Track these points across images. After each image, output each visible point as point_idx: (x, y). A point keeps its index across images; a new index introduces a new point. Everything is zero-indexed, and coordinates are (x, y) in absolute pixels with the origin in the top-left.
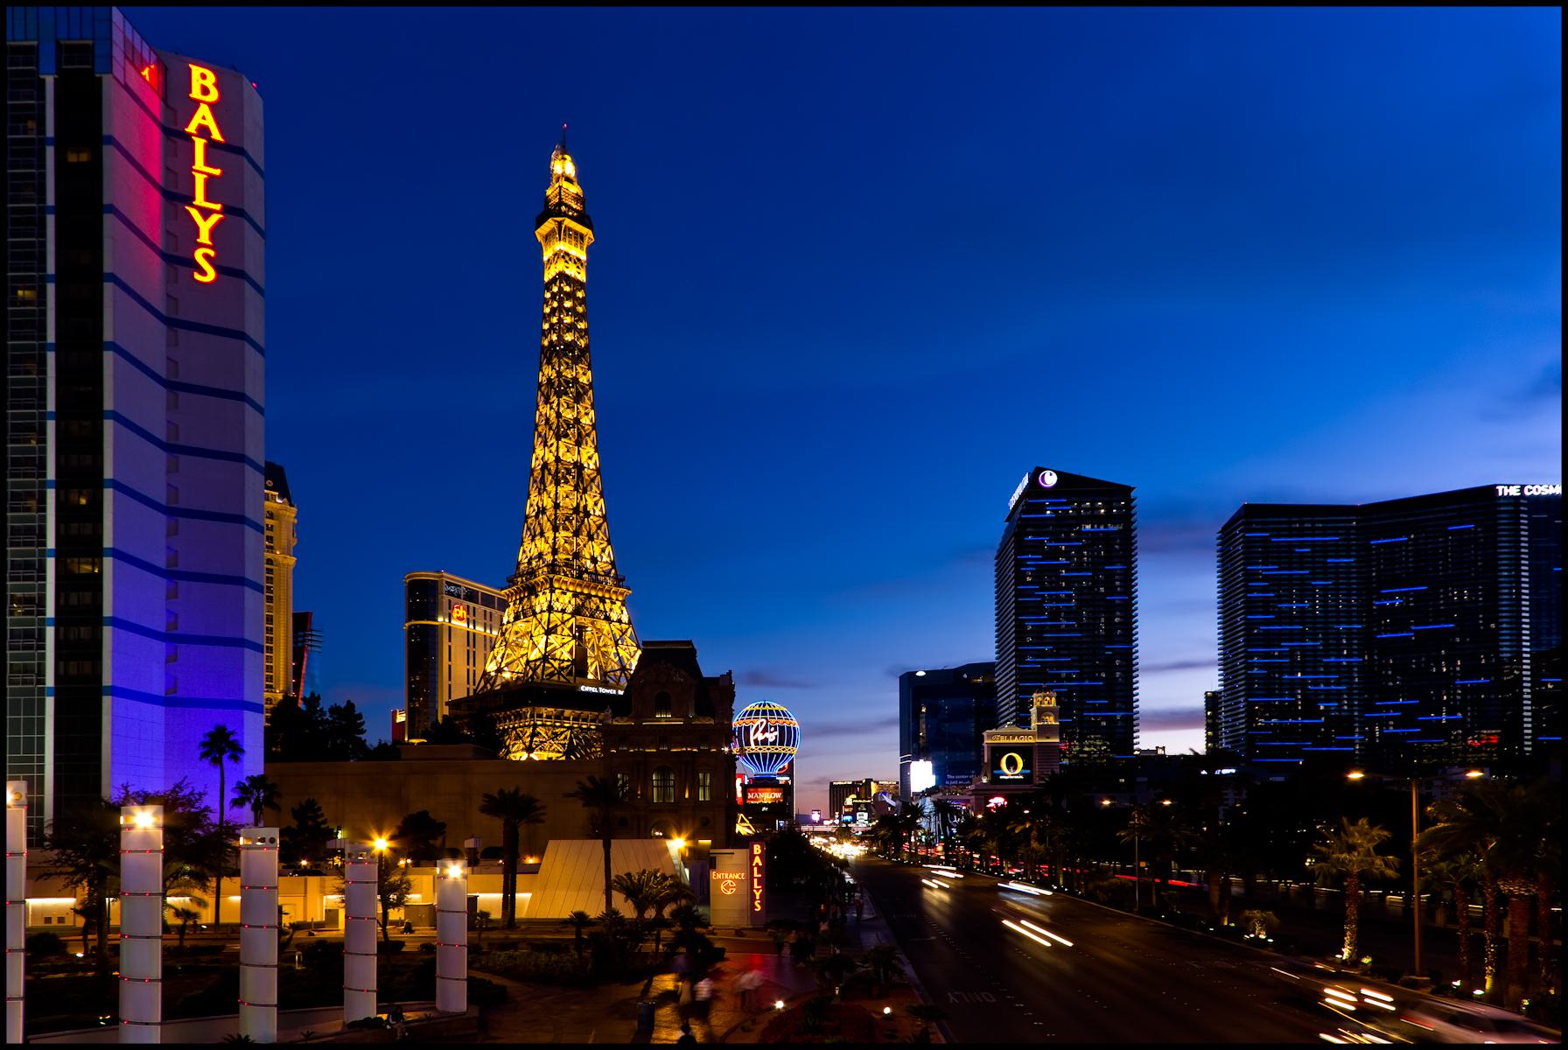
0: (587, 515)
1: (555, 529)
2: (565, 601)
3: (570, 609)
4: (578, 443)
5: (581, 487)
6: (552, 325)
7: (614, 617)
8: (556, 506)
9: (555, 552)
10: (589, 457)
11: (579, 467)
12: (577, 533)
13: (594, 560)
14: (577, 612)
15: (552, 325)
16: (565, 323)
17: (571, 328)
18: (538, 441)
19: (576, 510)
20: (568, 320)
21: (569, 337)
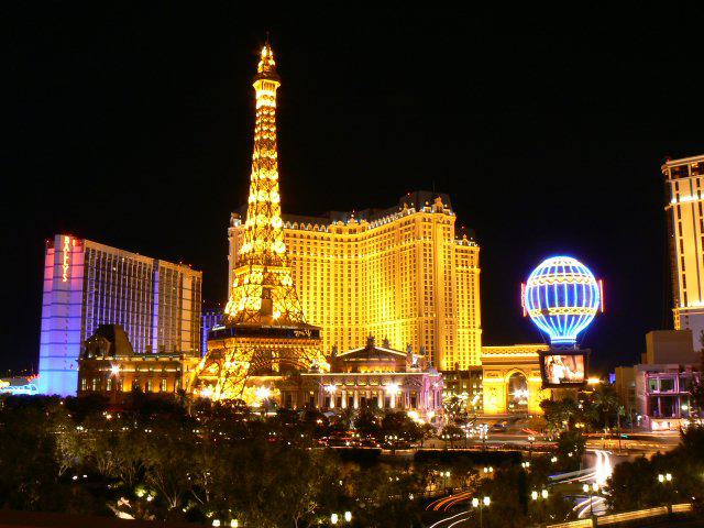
0: (272, 228)
1: (255, 239)
2: (259, 278)
3: (260, 282)
4: (268, 191)
5: (269, 213)
7: (284, 283)
8: (256, 226)
9: (254, 251)
10: (275, 198)
11: (269, 204)
12: (266, 240)
13: (275, 253)
14: (263, 284)
16: (266, 130)
17: (268, 131)
18: (251, 190)
19: (266, 227)
20: (265, 128)
21: (265, 137)
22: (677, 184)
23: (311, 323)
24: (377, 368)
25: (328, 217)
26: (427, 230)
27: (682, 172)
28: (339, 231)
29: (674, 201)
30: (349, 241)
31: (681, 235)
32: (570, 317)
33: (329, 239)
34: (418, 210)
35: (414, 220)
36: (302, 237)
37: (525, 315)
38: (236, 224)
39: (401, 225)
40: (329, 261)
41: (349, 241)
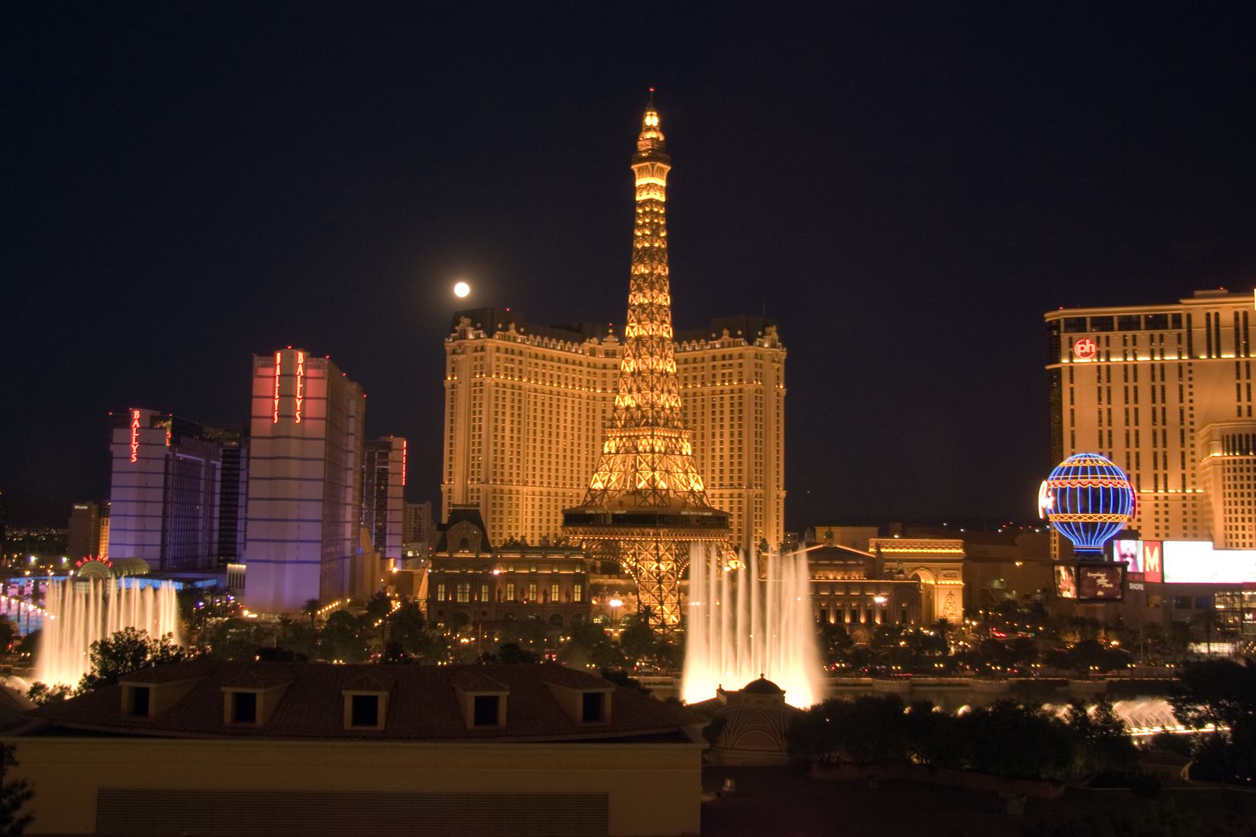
6: (644, 235)
15: (644, 235)
22: (1071, 339)
23: (717, 507)
24: (854, 574)
25: (579, 330)
26: (758, 370)
27: (1078, 325)
28: (593, 353)
29: (1065, 361)
30: (605, 367)
31: (1072, 403)
32: (1111, 524)
33: (581, 364)
34: (751, 342)
35: (741, 356)
36: (544, 358)
37: (1041, 516)
38: (471, 337)
39: (714, 358)
40: (580, 397)
41: (605, 367)
